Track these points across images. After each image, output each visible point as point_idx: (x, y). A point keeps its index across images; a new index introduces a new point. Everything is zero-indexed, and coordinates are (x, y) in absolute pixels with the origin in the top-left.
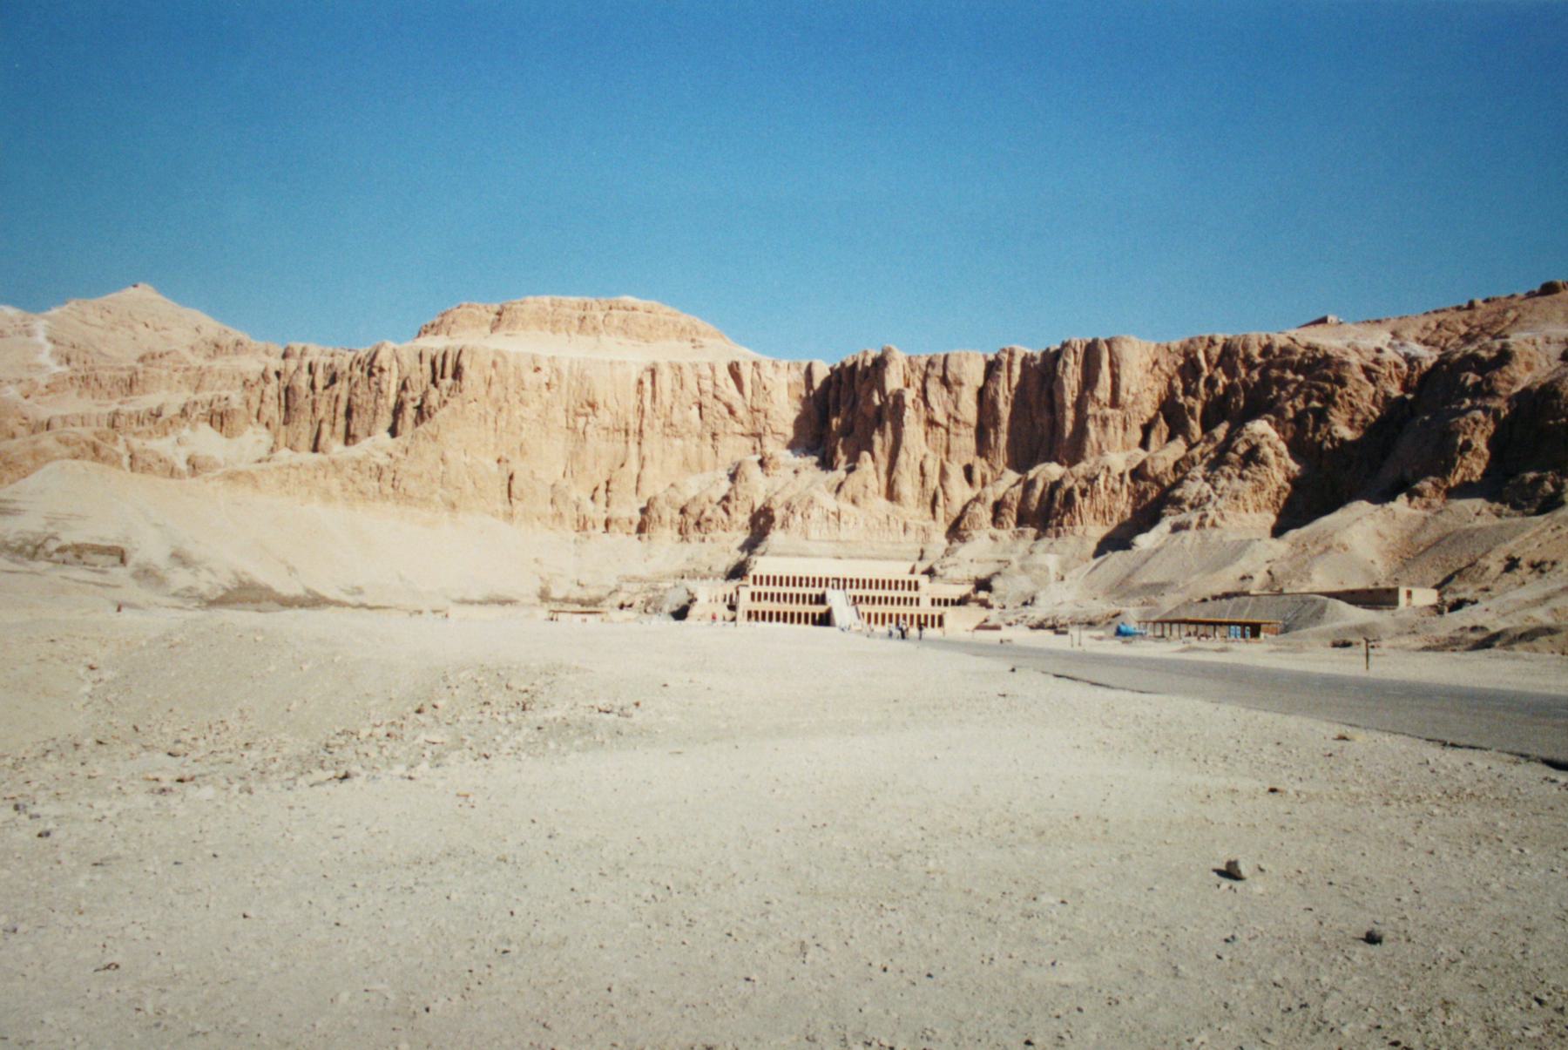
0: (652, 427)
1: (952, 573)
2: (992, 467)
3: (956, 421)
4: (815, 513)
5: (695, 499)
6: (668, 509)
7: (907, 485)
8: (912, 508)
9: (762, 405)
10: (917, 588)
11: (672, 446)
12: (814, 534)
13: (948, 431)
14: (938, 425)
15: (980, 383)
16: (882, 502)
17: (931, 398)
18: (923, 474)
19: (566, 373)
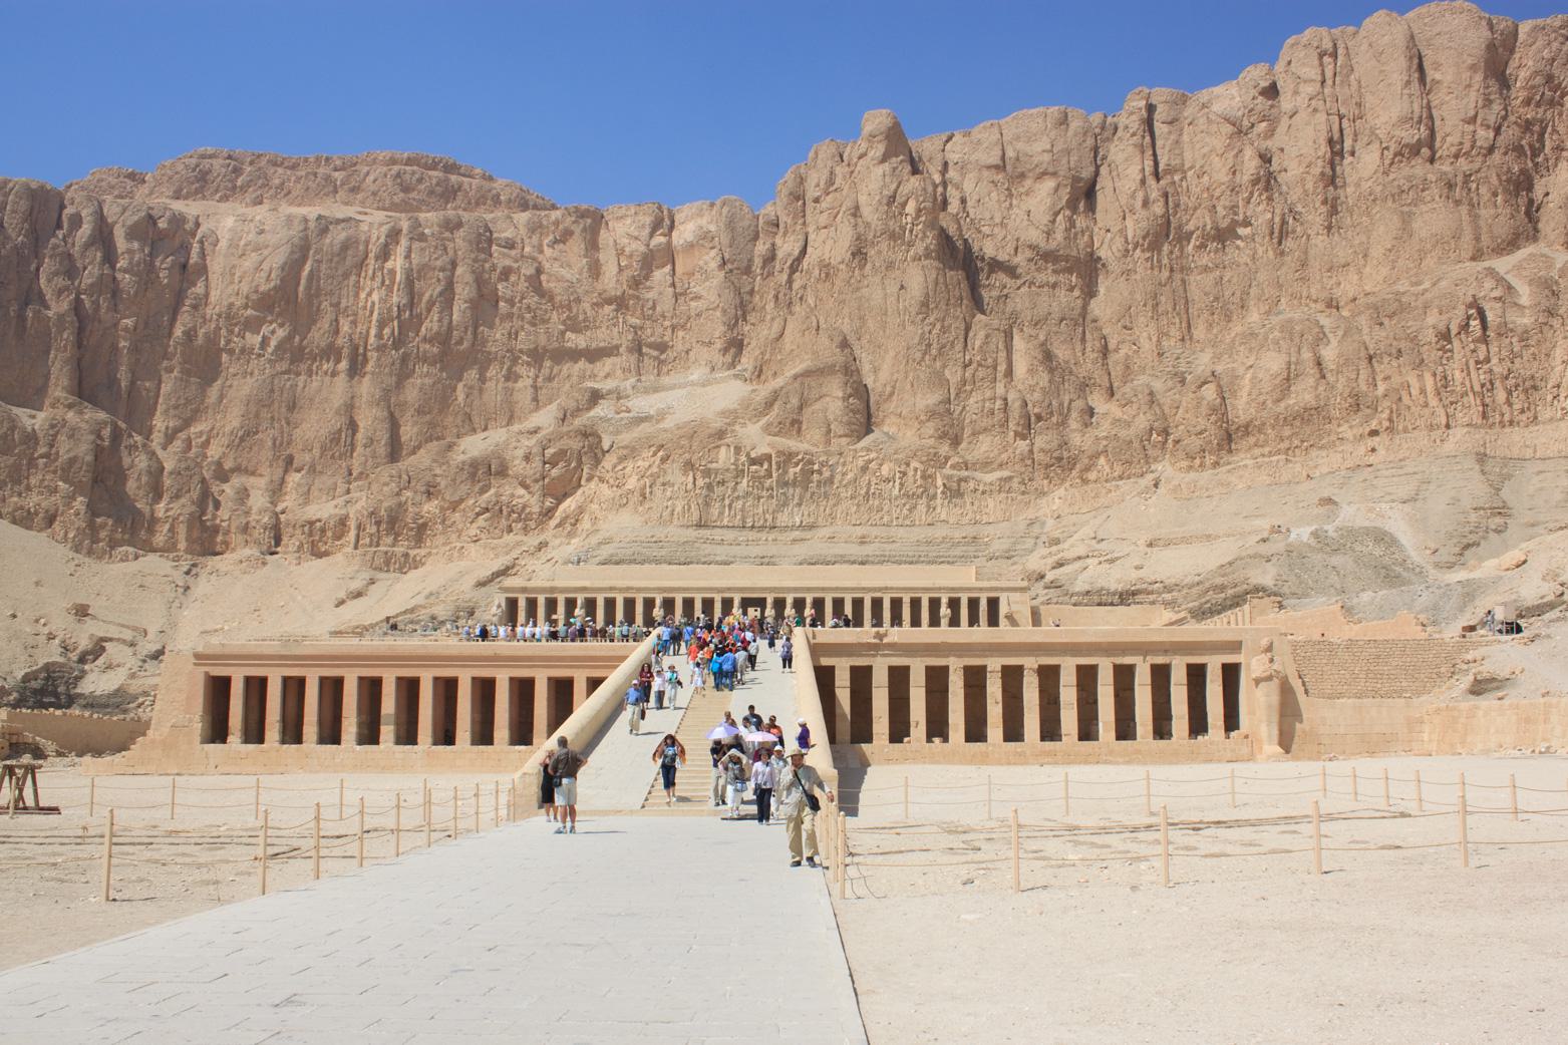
10: (993, 621)
19: (223, 244)
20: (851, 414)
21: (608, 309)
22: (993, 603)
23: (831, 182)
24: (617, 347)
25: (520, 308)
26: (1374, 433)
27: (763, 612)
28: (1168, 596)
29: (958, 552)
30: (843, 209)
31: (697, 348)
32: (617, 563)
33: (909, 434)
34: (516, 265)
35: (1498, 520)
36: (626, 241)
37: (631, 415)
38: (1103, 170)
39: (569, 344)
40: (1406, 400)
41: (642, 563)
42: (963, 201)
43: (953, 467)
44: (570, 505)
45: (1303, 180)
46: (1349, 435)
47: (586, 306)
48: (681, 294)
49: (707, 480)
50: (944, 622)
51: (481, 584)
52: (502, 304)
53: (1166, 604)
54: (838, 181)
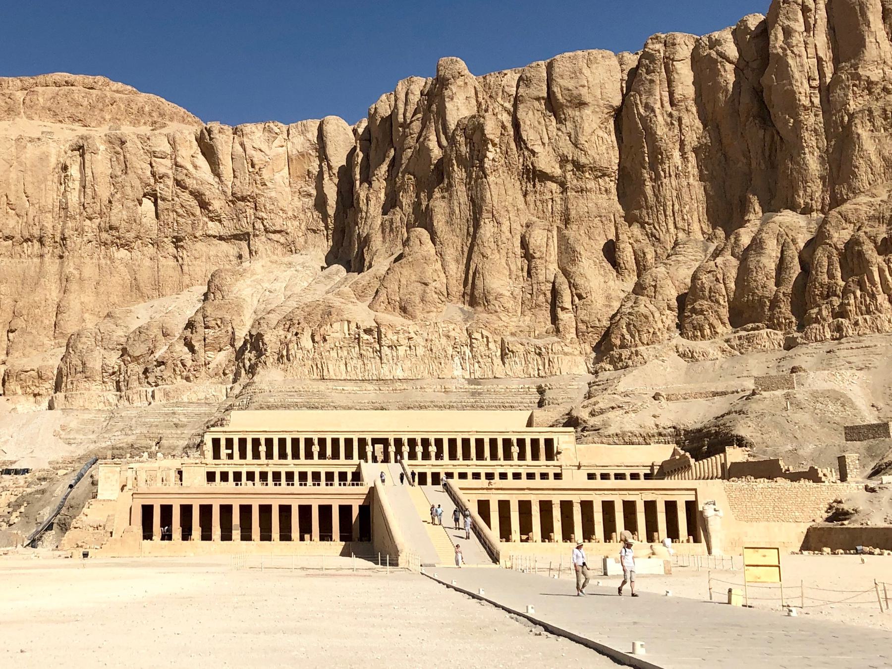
0: (80, 232)
1: (617, 422)
2: (654, 238)
3: (579, 167)
4: (337, 332)
5: (140, 331)
6: (98, 353)
7: (501, 278)
8: (512, 320)
9: (247, 190)
11: (112, 260)
12: (335, 369)
13: (563, 185)
14: (544, 177)
15: (617, 101)
16: (455, 309)
17: (528, 134)
18: (528, 256)
20: (436, 296)
21: (241, 204)
24: (248, 234)
25: (173, 205)
29: (519, 400)
31: (310, 235)
32: (269, 408)
33: (480, 309)
34: (170, 172)
36: (253, 153)
39: (210, 232)
43: (513, 334)
47: (223, 203)
48: (295, 192)
49: (333, 346)
50: (515, 455)
52: (159, 201)
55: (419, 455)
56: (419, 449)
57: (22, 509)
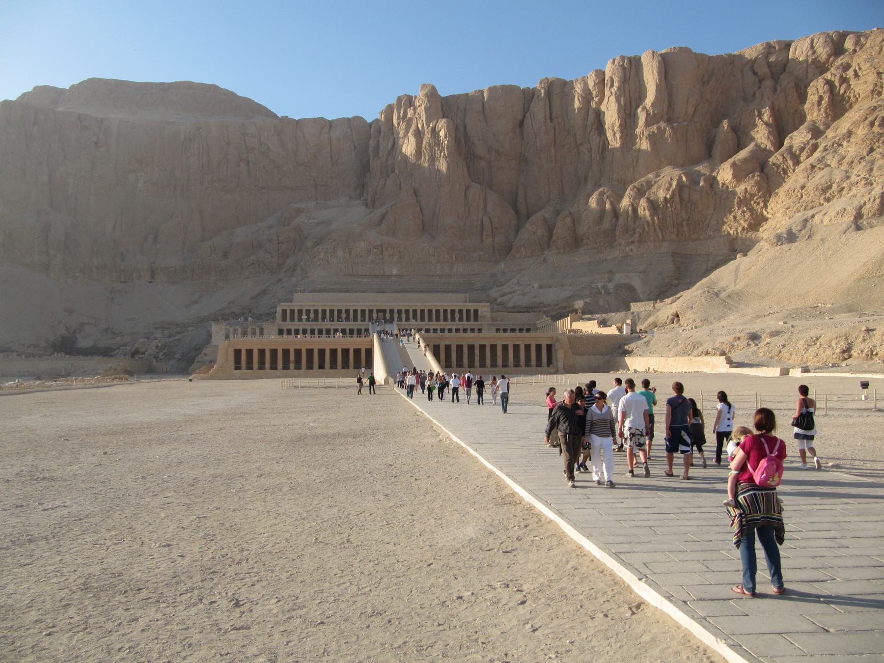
10: (476, 319)
22: (476, 311)
23: (405, 114)
26: (633, 242)
27: (384, 316)
28: (545, 309)
30: (411, 130)
35: (676, 282)
37: (316, 221)
38: (528, 115)
40: (646, 228)
41: (329, 291)
42: (465, 127)
44: (290, 262)
45: (613, 127)
46: (623, 242)
50: (457, 319)
51: (252, 298)
53: (544, 312)
54: (409, 116)
55: (404, 319)
56: (404, 316)
57: (166, 351)
